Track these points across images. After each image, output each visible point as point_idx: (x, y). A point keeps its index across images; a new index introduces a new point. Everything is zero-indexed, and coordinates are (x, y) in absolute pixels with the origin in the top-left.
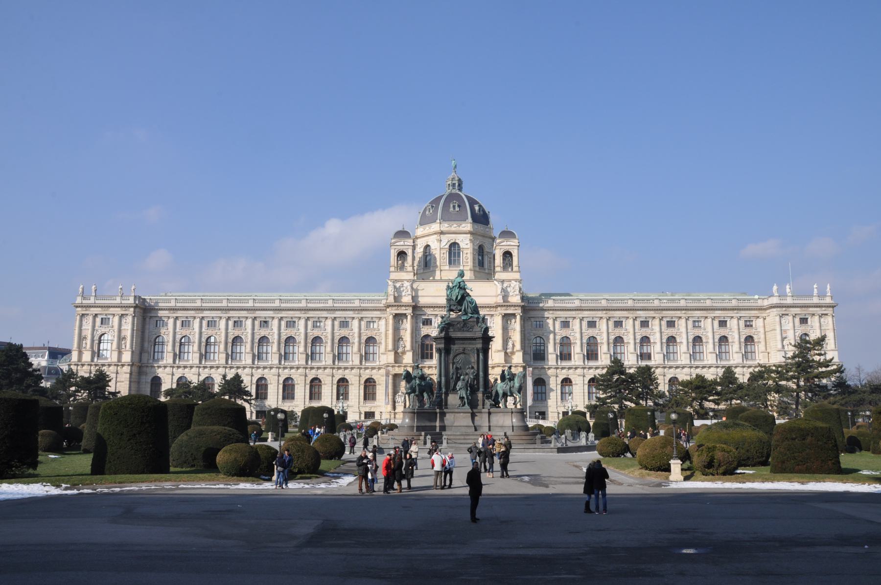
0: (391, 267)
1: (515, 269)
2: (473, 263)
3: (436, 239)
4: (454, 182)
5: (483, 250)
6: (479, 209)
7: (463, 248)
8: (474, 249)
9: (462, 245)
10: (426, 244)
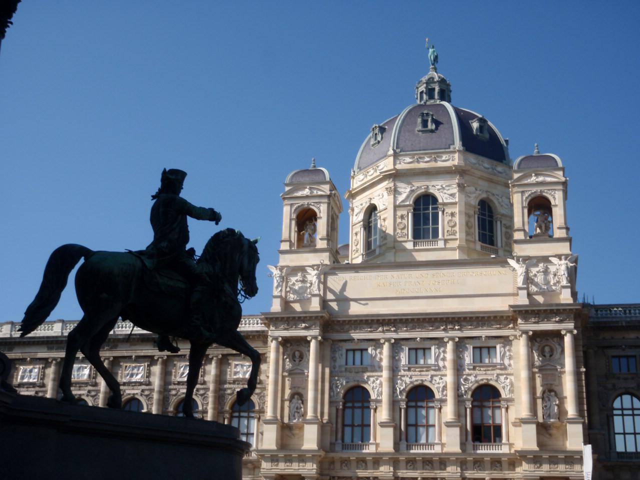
0: (282, 241)
1: (558, 233)
3: (387, 189)
4: (433, 86)
5: (490, 210)
6: (481, 128)
8: (467, 205)
9: (442, 197)
10: (368, 204)
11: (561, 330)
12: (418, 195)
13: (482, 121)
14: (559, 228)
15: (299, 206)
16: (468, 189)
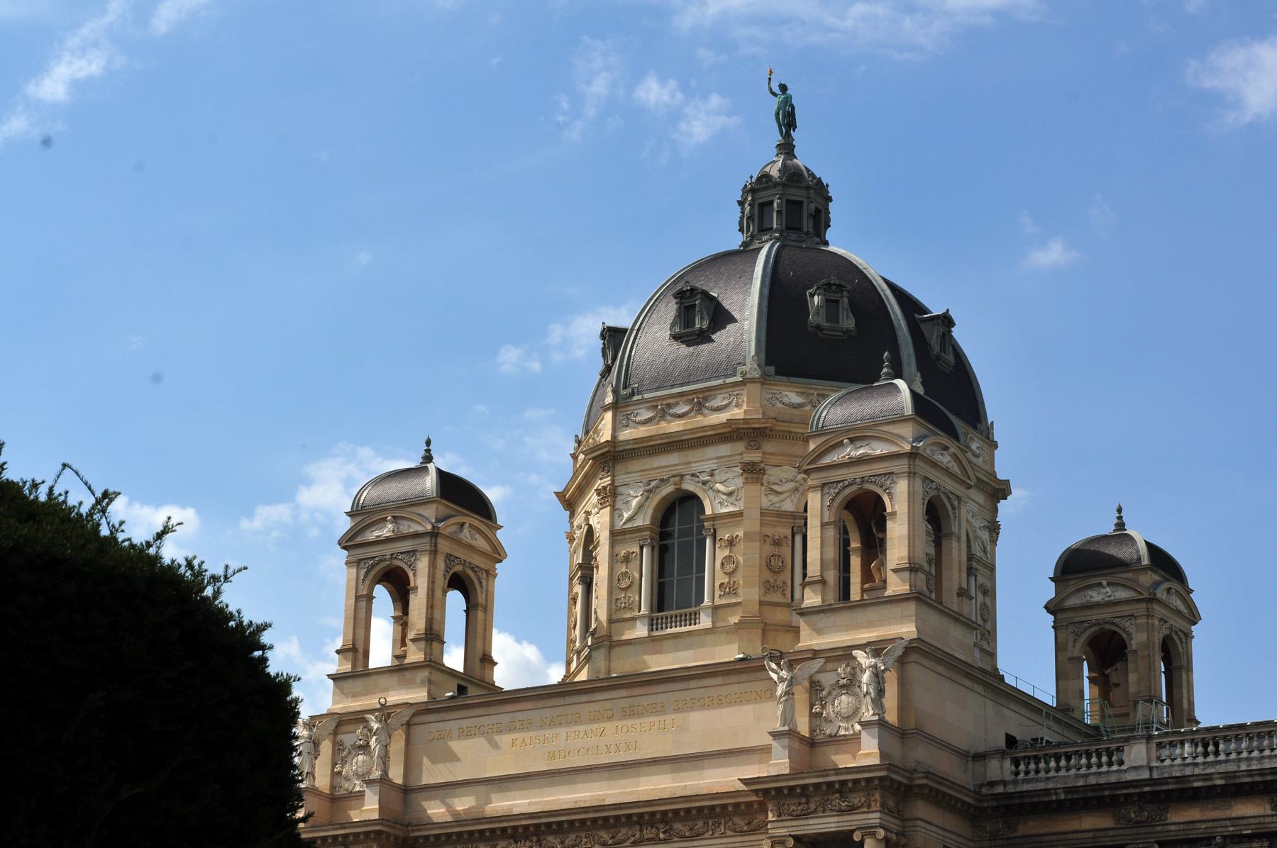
1: (896, 585)
2: (768, 587)
4: (763, 197)
7: (715, 518)
11: (854, 830)
12: (664, 499)
13: (834, 288)
14: (895, 571)
15: (373, 566)
16: (773, 474)
